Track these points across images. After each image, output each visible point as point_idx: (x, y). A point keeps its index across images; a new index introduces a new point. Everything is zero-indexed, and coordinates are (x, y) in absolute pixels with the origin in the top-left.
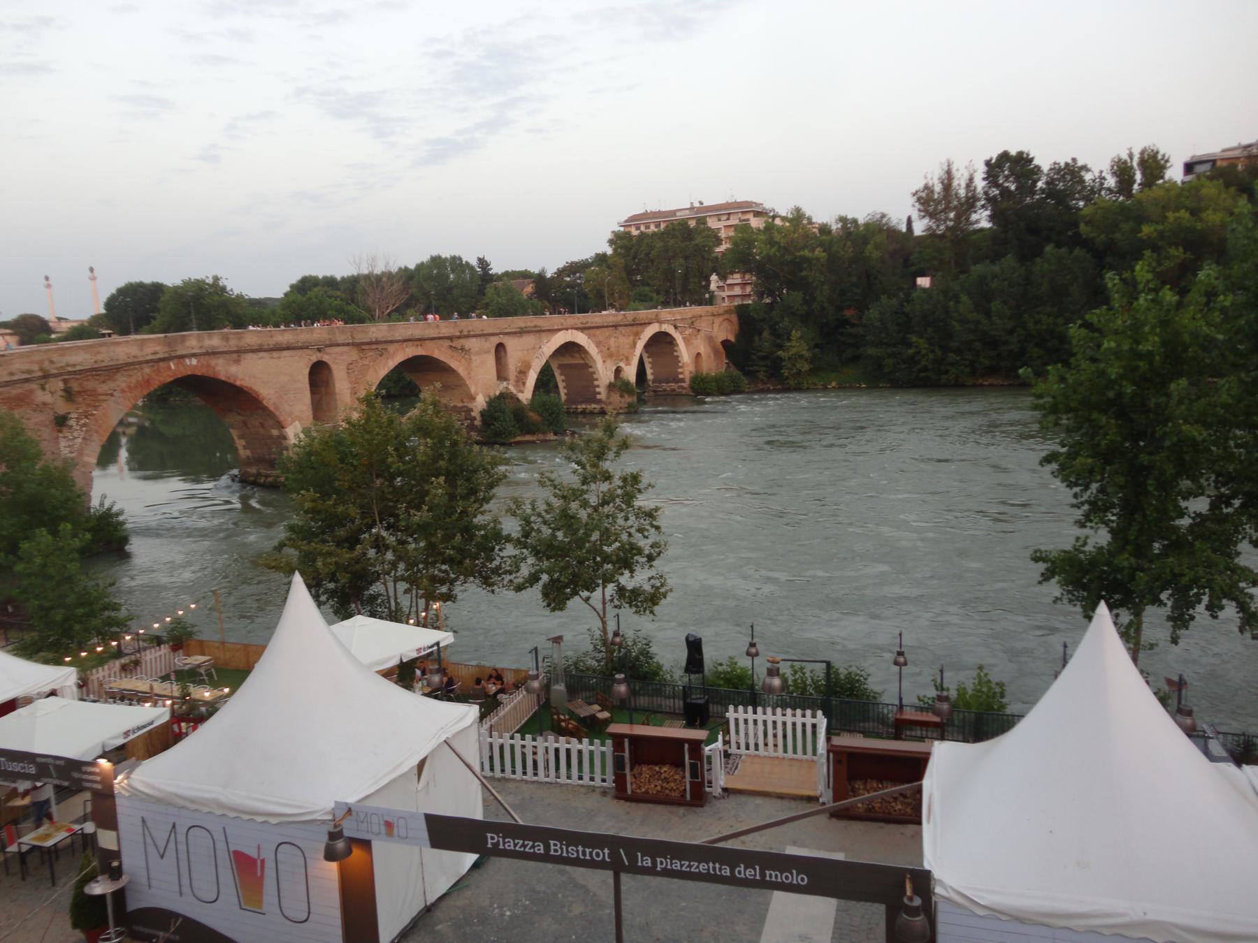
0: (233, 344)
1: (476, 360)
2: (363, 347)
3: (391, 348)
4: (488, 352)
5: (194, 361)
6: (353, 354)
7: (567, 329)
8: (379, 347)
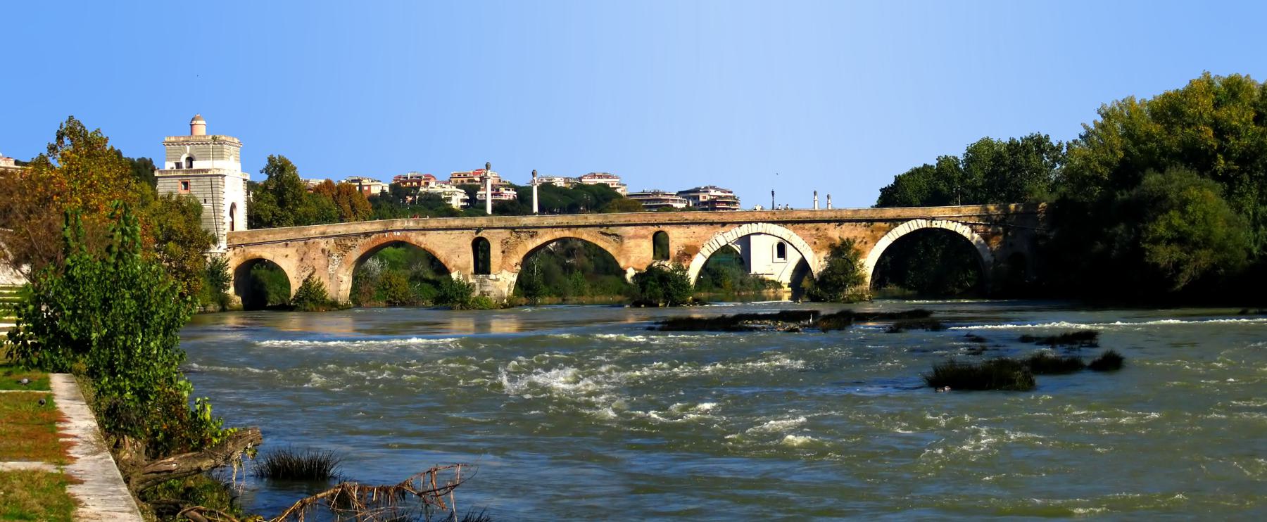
0: (421, 225)
1: (629, 244)
2: (517, 230)
3: (540, 231)
4: (645, 237)
5: (398, 233)
6: (505, 234)
7: (751, 222)
8: (532, 231)
